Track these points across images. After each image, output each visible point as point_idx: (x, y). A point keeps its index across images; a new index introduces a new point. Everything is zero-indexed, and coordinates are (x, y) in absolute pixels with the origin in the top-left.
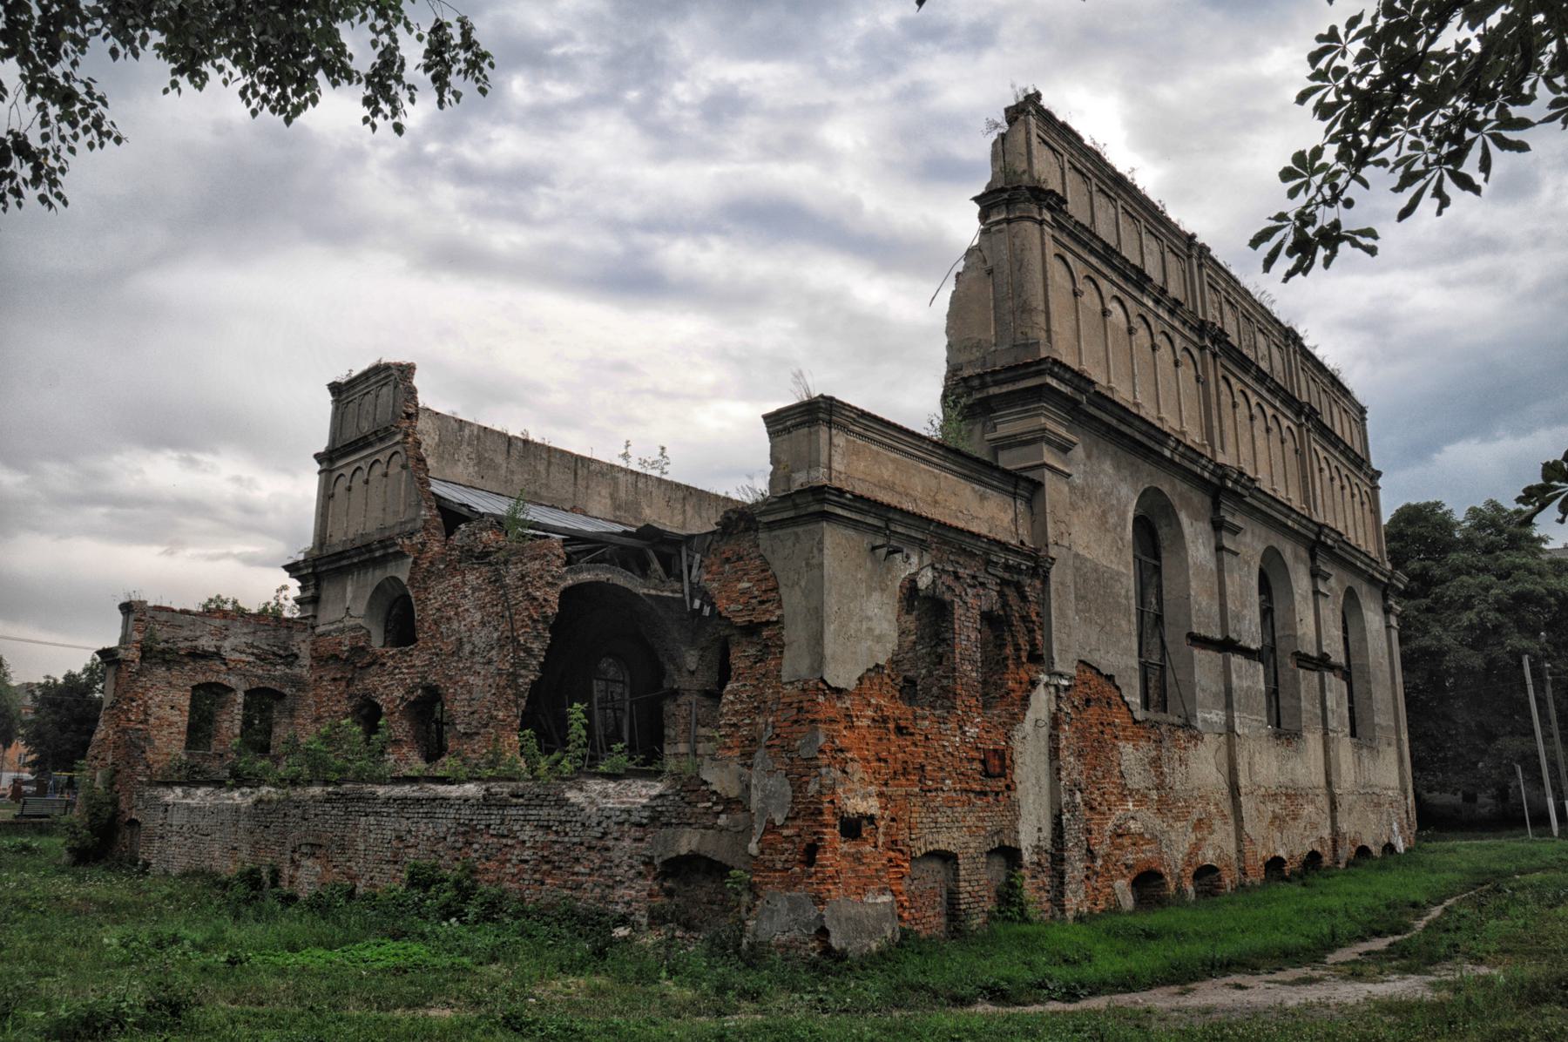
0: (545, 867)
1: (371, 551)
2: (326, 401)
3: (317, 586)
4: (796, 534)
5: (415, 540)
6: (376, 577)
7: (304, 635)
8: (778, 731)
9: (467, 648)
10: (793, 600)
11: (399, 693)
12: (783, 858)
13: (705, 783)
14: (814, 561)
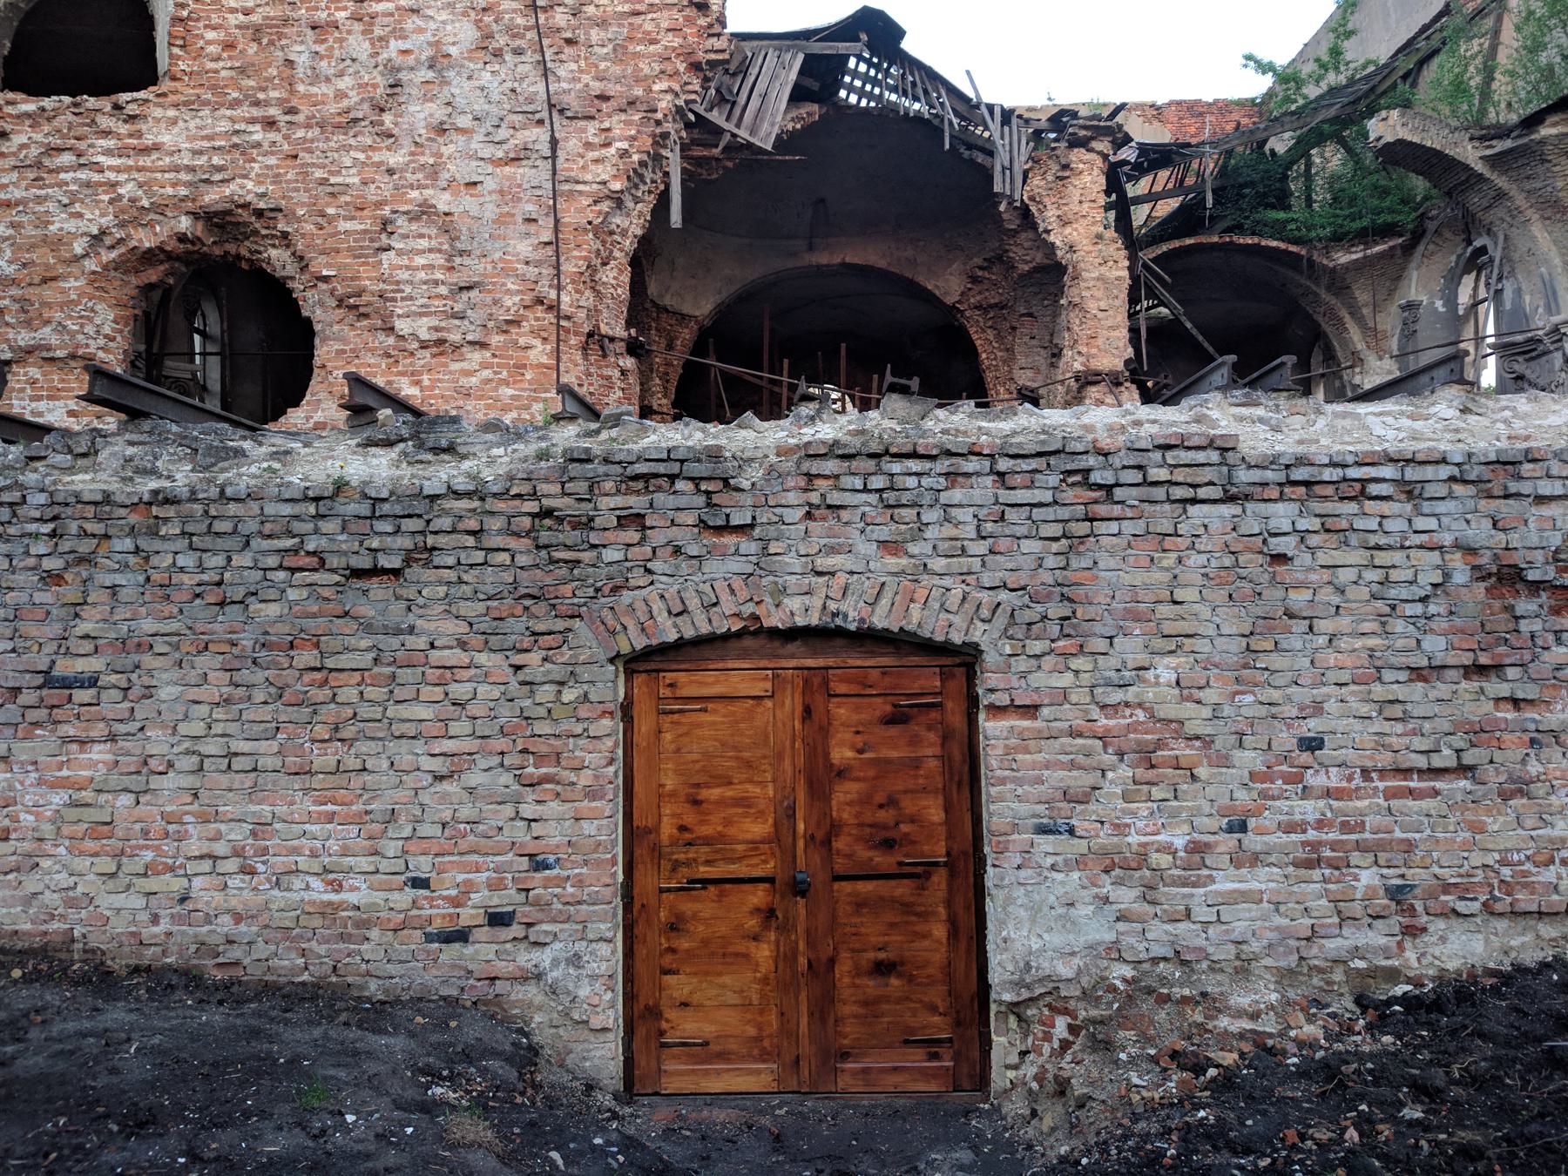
9: (419, 114)
11: (96, 218)
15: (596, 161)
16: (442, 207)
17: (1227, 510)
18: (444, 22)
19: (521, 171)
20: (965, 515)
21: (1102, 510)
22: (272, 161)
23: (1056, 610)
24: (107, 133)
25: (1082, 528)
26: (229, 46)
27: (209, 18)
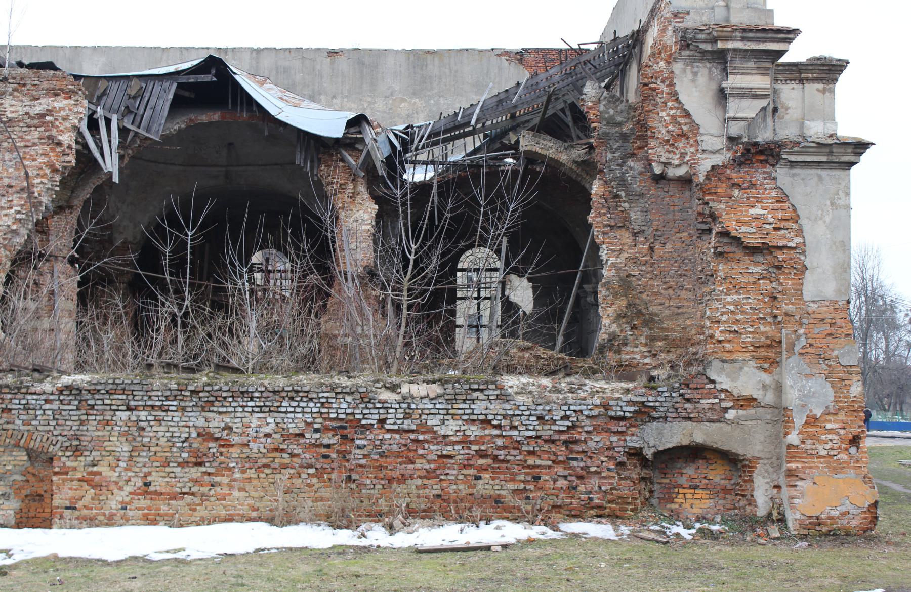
0: (481, 462)
4: (820, 178)
8: (812, 341)
10: (815, 231)
12: (828, 447)
13: (713, 382)
14: (841, 202)
15: (6, 215)
17: (128, 413)
20: (50, 413)
21: (91, 412)
23: (75, 443)
25: (84, 418)
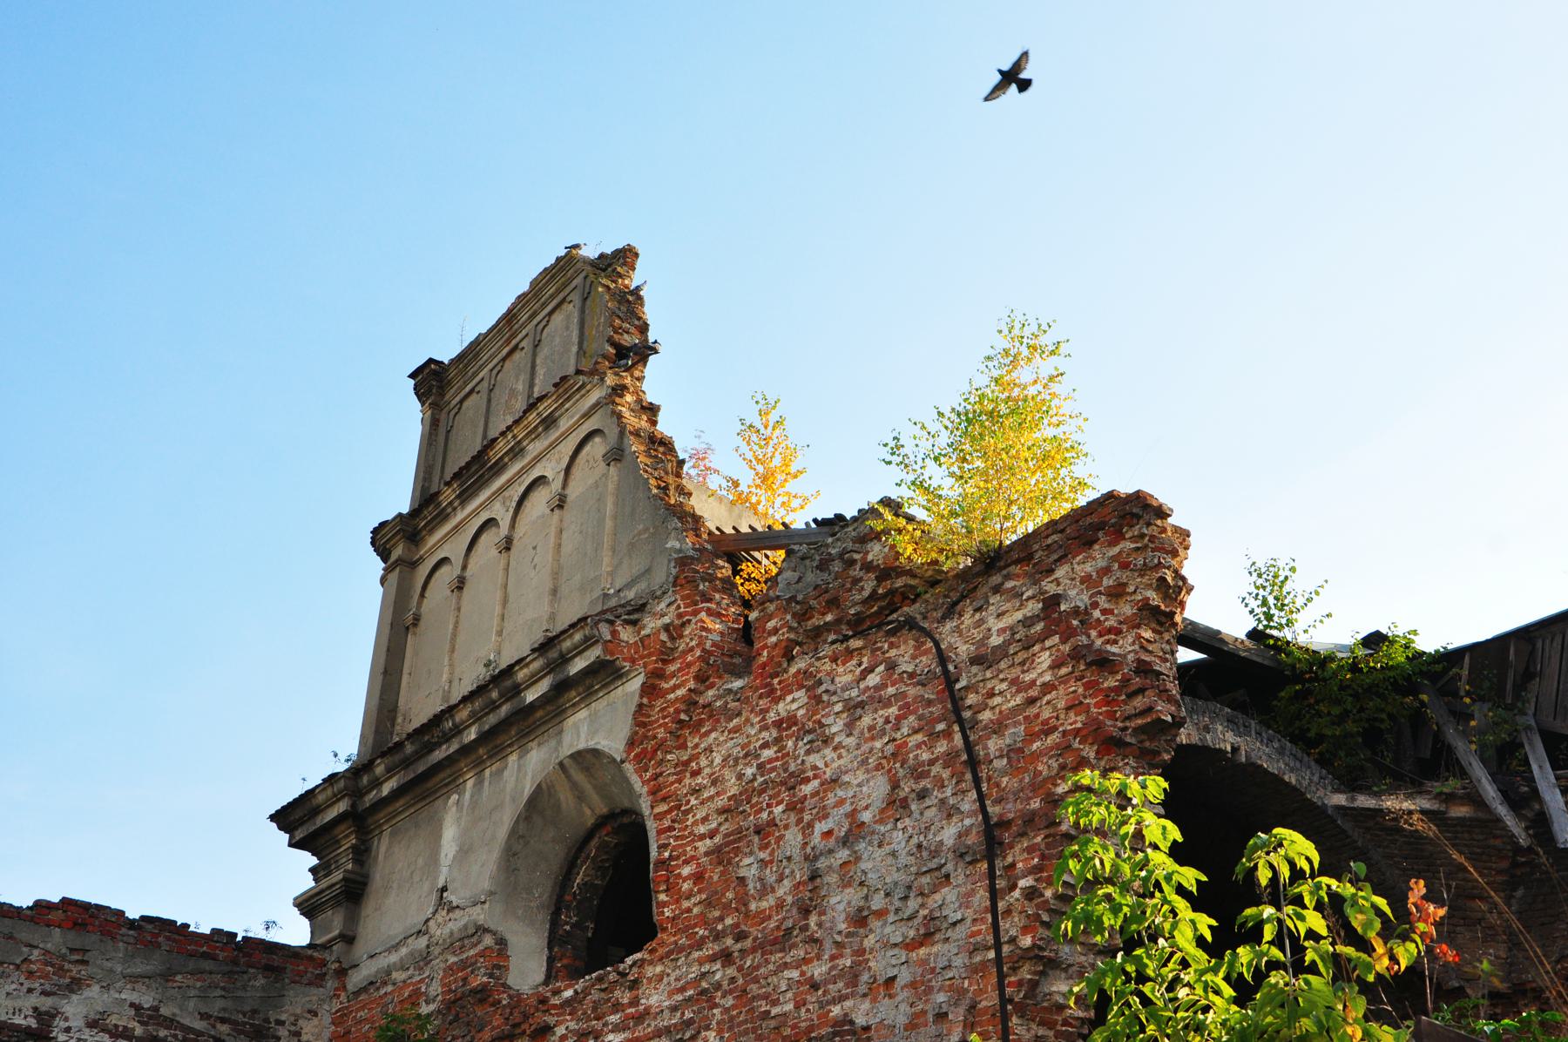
1: (517, 690)
2: (410, 416)
3: (362, 854)
5: (651, 624)
6: (528, 767)
7: (315, 994)
9: (841, 902)
16: (860, 1021)
18: (859, 785)
19: (935, 949)
22: (729, 1001)
24: (617, 1007)
26: (698, 877)
27: (685, 853)
